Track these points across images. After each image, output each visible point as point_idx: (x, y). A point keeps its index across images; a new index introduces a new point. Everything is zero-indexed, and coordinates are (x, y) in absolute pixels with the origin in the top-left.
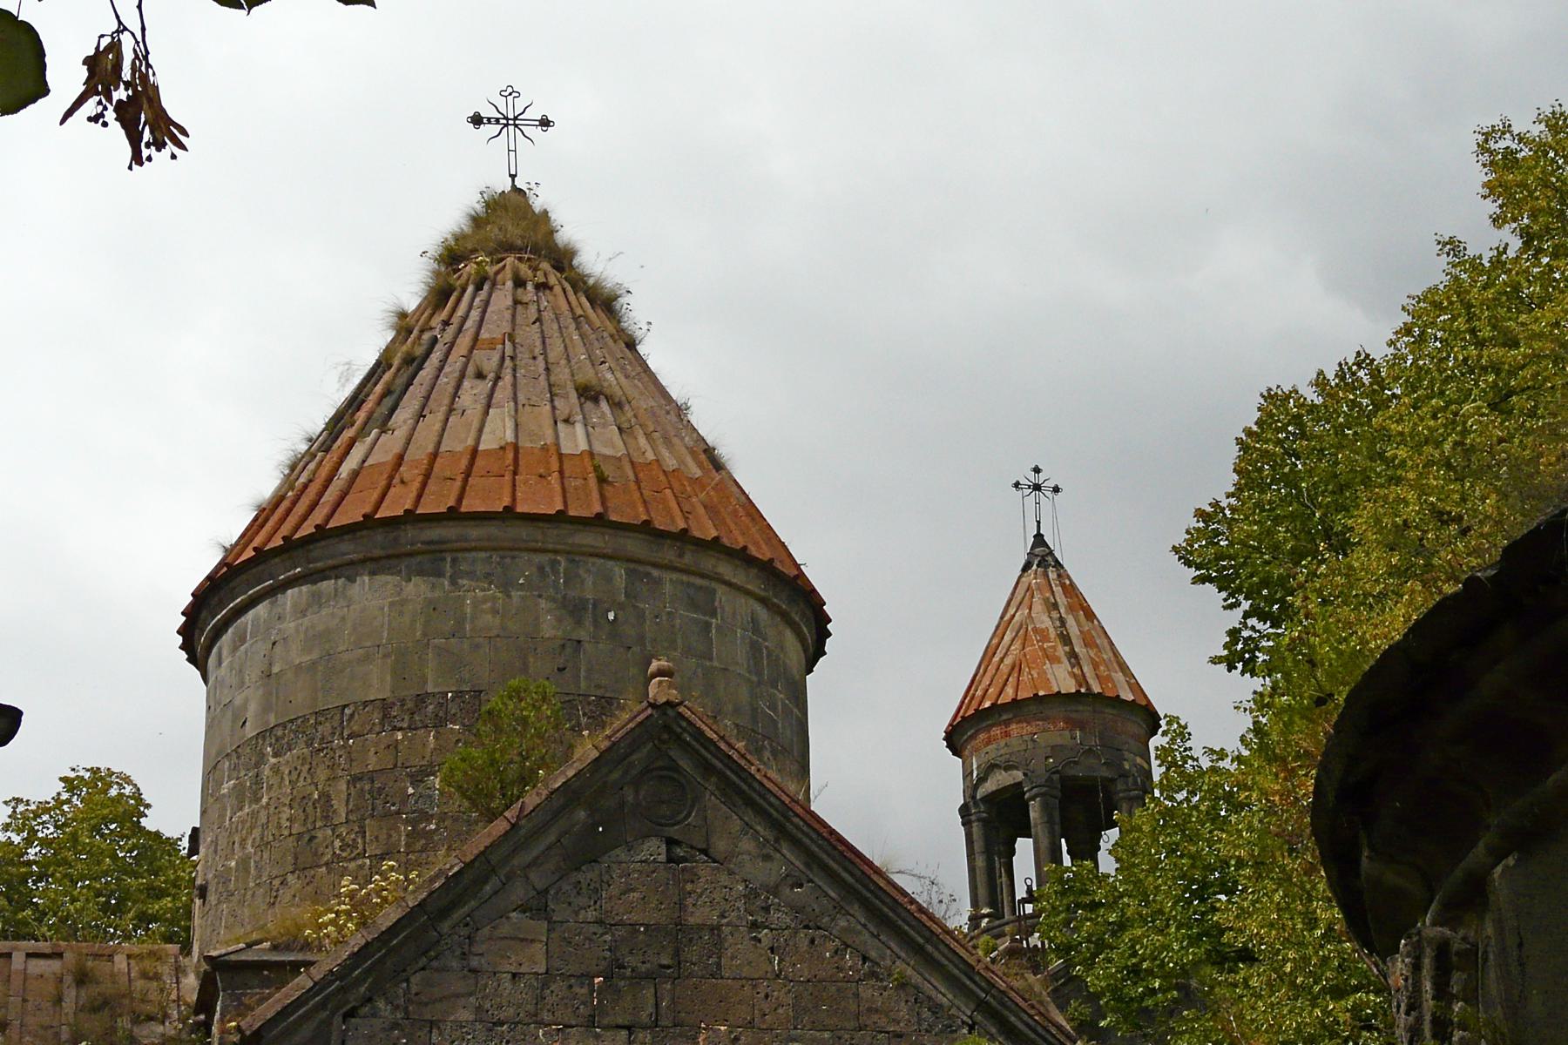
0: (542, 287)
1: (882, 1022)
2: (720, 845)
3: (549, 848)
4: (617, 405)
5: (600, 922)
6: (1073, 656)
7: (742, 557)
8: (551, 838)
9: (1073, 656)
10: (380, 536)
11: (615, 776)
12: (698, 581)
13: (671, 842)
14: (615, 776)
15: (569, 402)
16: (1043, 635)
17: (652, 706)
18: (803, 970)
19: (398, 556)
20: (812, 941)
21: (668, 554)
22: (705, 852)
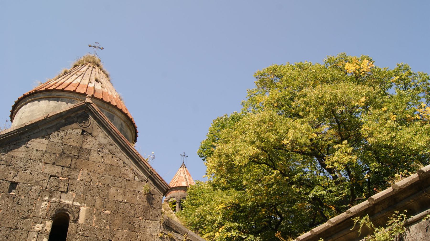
0: (94, 68)
1: (125, 177)
2: (94, 134)
3: (53, 126)
4: (101, 83)
5: (62, 143)
6: (186, 181)
7: (121, 111)
8: (55, 123)
9: (186, 181)
10: (48, 93)
11: (72, 115)
12: (111, 113)
13: (83, 131)
14: (72, 115)
15: (93, 81)
16: (182, 177)
17: (86, 103)
18: (109, 162)
19: (51, 98)
20: (112, 157)
21: (106, 106)
22: (91, 134)
